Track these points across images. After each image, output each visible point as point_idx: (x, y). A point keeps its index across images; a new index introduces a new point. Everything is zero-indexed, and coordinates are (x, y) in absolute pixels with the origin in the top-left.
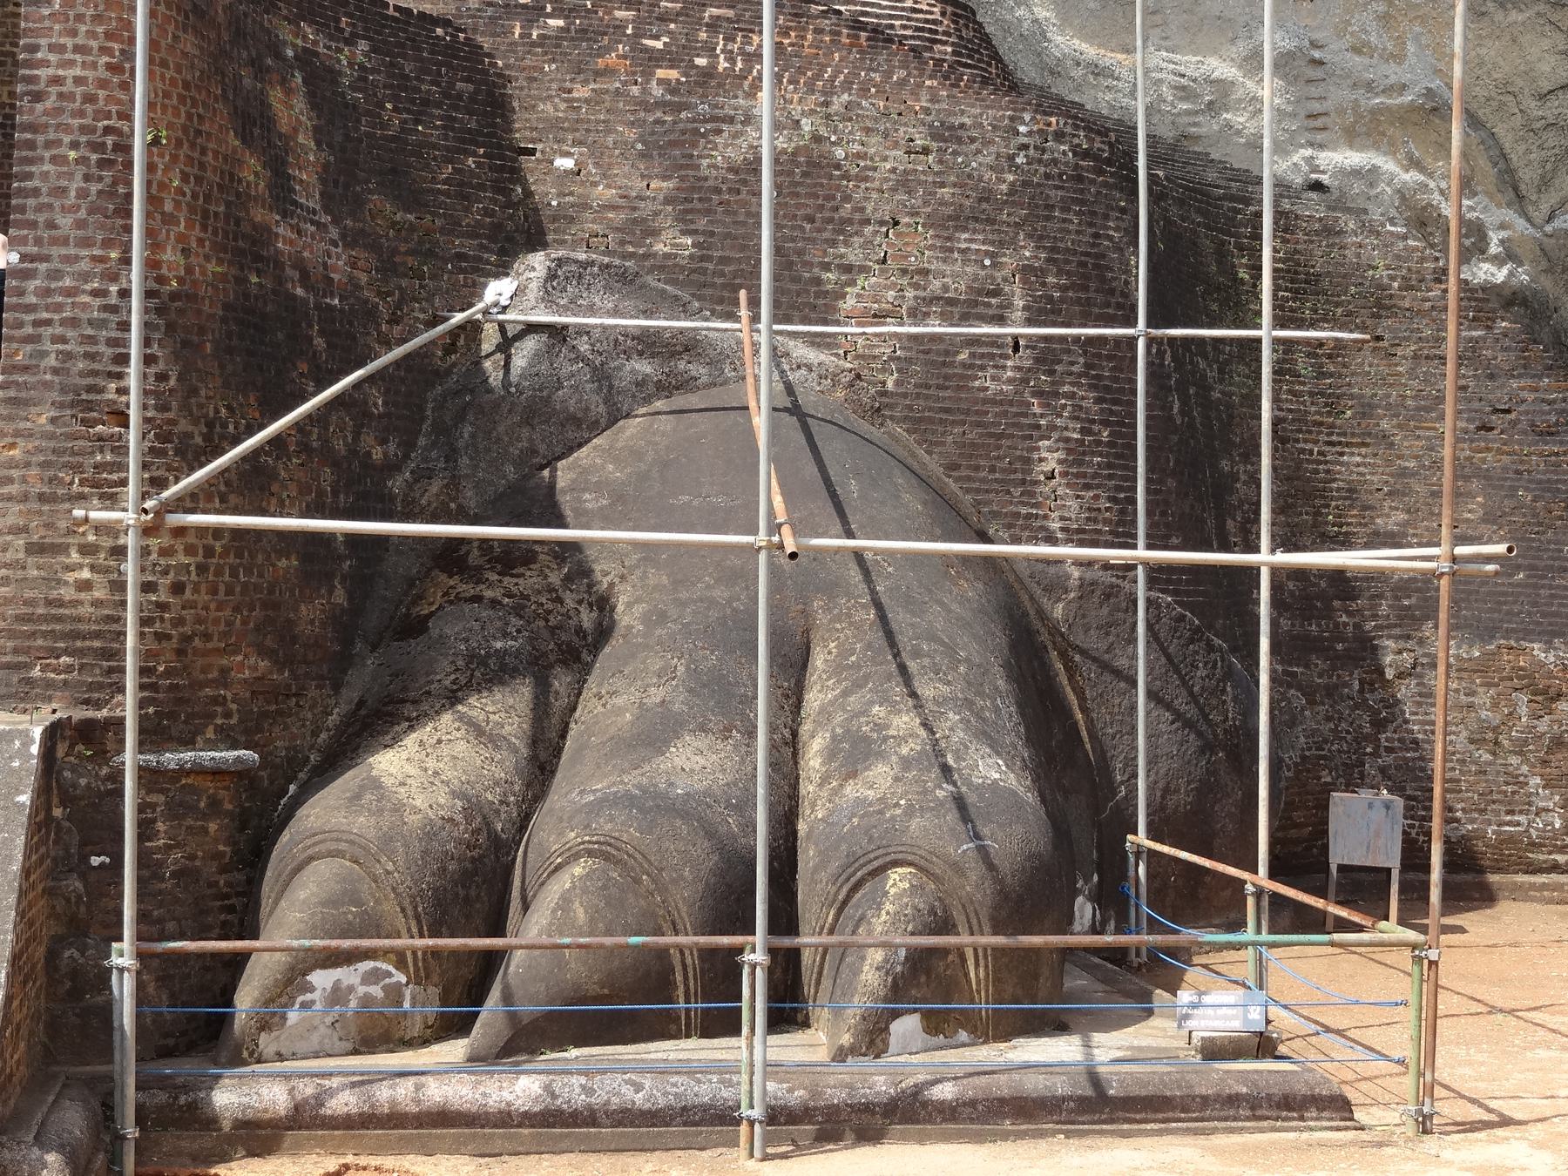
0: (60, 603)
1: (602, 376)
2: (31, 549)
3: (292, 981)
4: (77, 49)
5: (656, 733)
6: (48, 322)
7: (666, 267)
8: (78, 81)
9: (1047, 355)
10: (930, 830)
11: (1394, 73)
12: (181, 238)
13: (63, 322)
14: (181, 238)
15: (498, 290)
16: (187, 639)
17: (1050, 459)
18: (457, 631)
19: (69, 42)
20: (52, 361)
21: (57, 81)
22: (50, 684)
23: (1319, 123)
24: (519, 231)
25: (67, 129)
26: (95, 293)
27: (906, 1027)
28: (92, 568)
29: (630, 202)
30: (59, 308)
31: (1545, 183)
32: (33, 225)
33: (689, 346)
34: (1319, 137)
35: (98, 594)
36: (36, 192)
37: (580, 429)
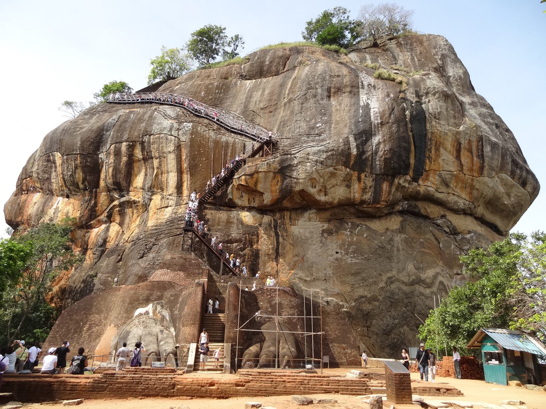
1: (264, 320)
3: (246, 362)
5: (269, 346)
7: (269, 311)
9: (298, 318)
10: (288, 353)
11: (334, 290)
15: (257, 314)
17: (299, 327)
18: (254, 339)
24: (258, 309)
27: (287, 367)
29: (266, 306)
31: (350, 301)
33: (271, 318)
37: (263, 324)
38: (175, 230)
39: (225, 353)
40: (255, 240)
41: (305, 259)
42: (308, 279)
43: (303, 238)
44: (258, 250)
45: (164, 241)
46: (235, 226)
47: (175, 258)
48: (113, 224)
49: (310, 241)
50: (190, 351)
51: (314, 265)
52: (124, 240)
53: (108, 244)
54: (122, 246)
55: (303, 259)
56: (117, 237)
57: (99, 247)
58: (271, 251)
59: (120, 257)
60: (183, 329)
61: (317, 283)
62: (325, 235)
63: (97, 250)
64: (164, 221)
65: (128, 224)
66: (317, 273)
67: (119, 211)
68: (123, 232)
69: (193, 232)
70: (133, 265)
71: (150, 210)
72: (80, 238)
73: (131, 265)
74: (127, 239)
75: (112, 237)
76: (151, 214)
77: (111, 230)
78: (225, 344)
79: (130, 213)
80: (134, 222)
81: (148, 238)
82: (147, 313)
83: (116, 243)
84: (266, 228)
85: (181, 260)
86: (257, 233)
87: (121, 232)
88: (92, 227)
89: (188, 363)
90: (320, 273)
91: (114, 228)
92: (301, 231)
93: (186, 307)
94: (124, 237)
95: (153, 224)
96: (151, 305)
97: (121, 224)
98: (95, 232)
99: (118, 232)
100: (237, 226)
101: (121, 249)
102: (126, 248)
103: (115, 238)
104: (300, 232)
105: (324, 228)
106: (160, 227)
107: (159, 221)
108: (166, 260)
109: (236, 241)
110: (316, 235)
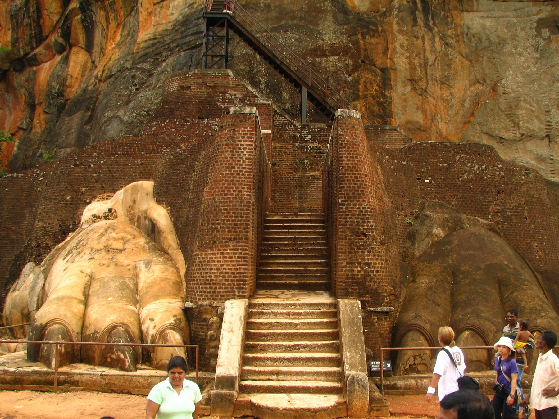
0: (354, 275)
2: (347, 263)
4: (351, 157)
6: (348, 215)
8: (352, 164)
12: (372, 196)
13: (351, 215)
14: (372, 196)
16: (379, 283)
19: (349, 156)
20: (349, 223)
21: (346, 164)
22: (353, 293)
23: (553, 172)
25: (350, 174)
26: (358, 208)
28: (360, 268)
30: (350, 211)
32: (344, 194)
34: (553, 175)
35: (362, 273)
36: (344, 187)
38: (192, 38)
39: (345, 331)
40: (380, 49)
41: (501, 91)
42: (505, 135)
43: (494, 39)
44: (386, 69)
45: (168, 63)
46: (329, 17)
47: (188, 88)
48: (74, 49)
49: (508, 48)
50: (224, 326)
51: (522, 104)
52: (96, 77)
53: (68, 90)
54: (93, 91)
55: (494, 89)
56: (82, 76)
57: (53, 99)
58: (419, 73)
59: (89, 113)
60: (199, 255)
61: (530, 145)
62: (546, 33)
63: (50, 104)
64: (169, 26)
65: (101, 44)
66: (528, 122)
67: (83, 21)
68: (93, 62)
69: (231, 26)
70: (110, 120)
71: (141, 9)
72: (22, 87)
73: (106, 122)
74: (100, 74)
75: (75, 75)
76: (143, 16)
77: (71, 64)
78: (342, 302)
79: (103, 21)
80: (113, 39)
81: (138, 63)
82: (110, 214)
83: (83, 86)
84: (402, 19)
85: (203, 90)
86: (383, 31)
87: (89, 65)
88: (38, 62)
89: (220, 371)
90: (536, 122)
91: (78, 58)
92: (489, 23)
93: (207, 189)
94: (95, 73)
95: (147, 37)
96: (120, 193)
97: (89, 48)
98: (45, 72)
99: (85, 66)
100: (334, 17)
101: (91, 97)
102: (100, 93)
103: (80, 77)
104: (484, 27)
105: (542, 15)
106: (161, 40)
107: (160, 29)
108: (169, 94)
109: (334, 50)
110: (523, 34)
